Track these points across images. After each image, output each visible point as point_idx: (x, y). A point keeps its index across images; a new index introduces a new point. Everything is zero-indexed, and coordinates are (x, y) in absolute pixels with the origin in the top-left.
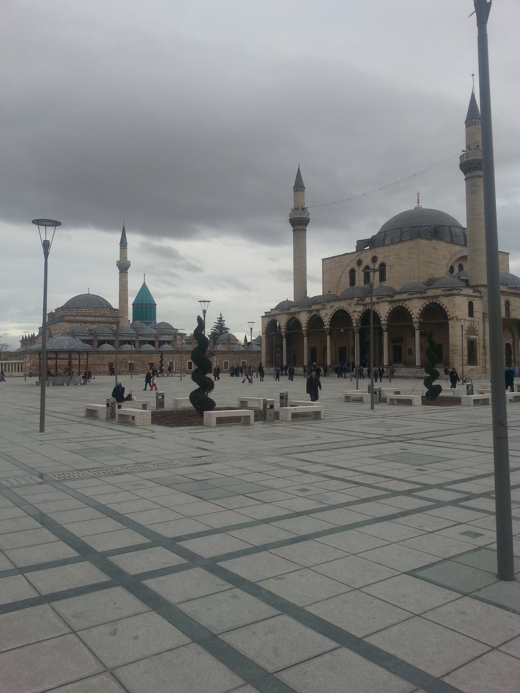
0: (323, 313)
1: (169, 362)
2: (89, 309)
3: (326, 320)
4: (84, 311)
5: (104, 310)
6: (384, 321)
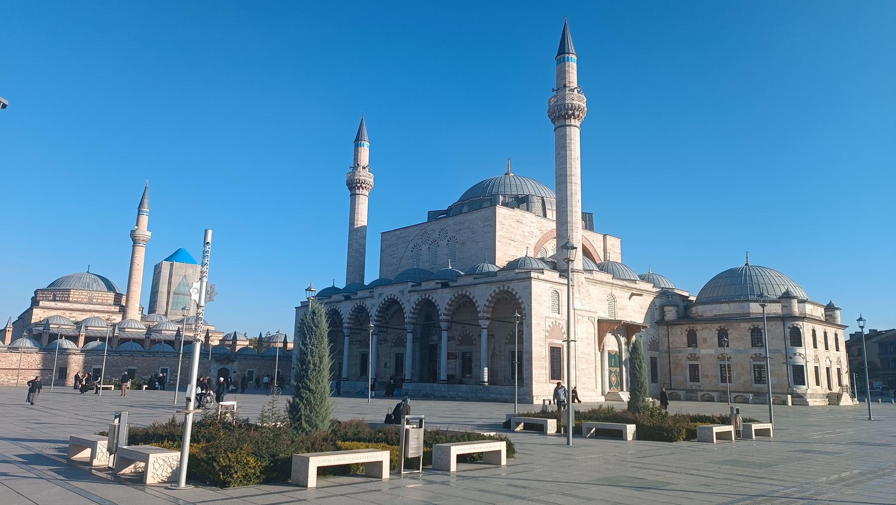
0: (368, 303)
1: (160, 369)
2: (81, 293)
3: (373, 312)
4: (72, 296)
5: (103, 295)
6: (444, 315)
